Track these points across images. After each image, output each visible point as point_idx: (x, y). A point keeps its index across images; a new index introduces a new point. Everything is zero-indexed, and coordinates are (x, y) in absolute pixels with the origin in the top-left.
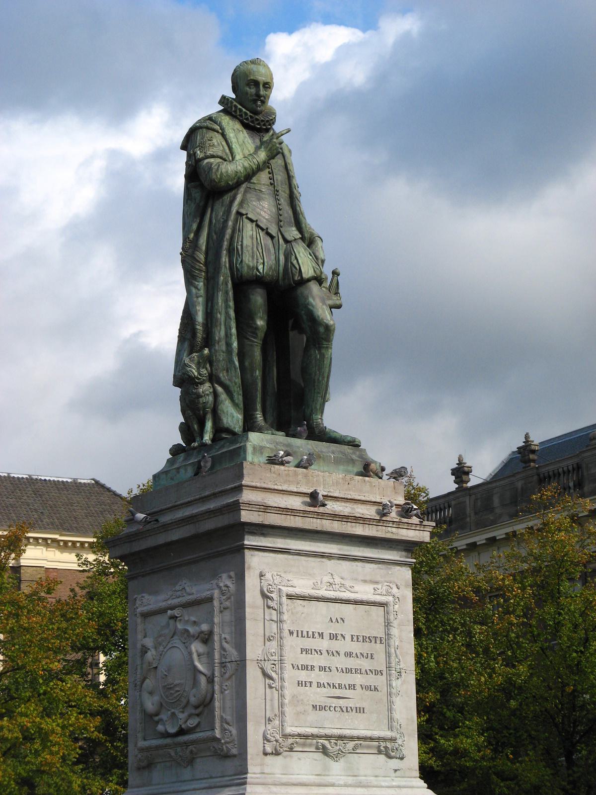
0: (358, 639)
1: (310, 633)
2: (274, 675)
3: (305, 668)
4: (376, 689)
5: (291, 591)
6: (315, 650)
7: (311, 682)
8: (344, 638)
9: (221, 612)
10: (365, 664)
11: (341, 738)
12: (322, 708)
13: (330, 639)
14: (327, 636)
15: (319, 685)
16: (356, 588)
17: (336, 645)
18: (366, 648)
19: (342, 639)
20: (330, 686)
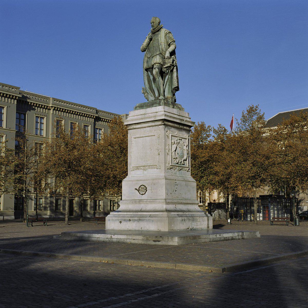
5: (135, 137)
11: (144, 166)
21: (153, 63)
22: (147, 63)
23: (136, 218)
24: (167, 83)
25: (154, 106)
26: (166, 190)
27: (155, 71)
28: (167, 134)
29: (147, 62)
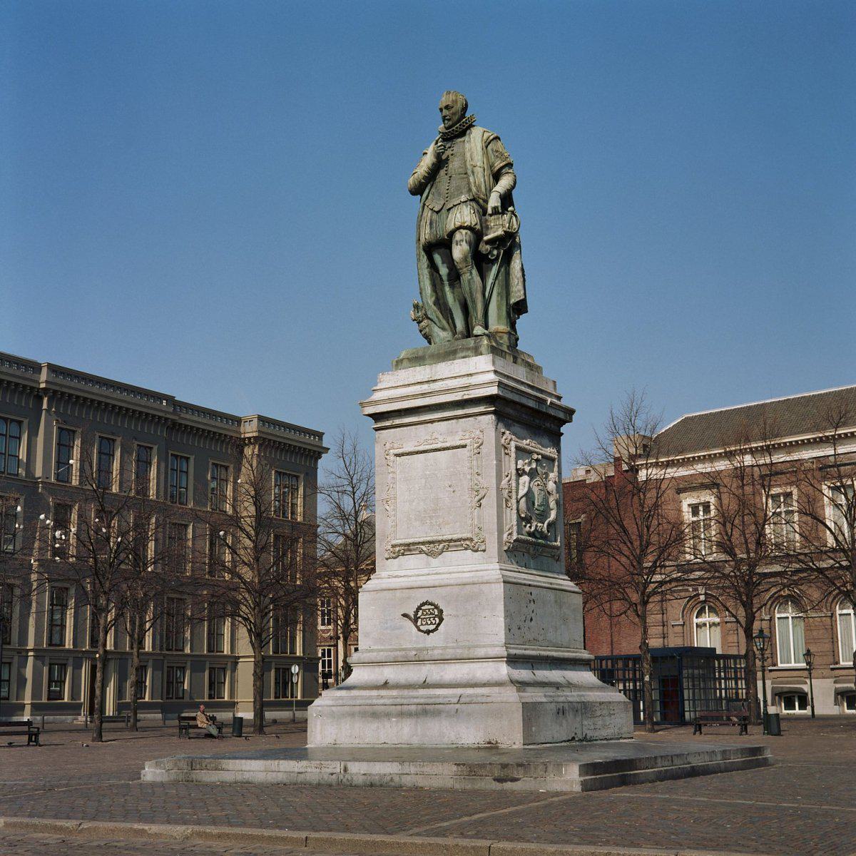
11: (430, 542)
21: (451, 227)
22: (431, 228)
23: (413, 708)
24: (495, 288)
25: (458, 356)
26: (506, 617)
27: (459, 251)
28: (503, 441)
29: (431, 224)
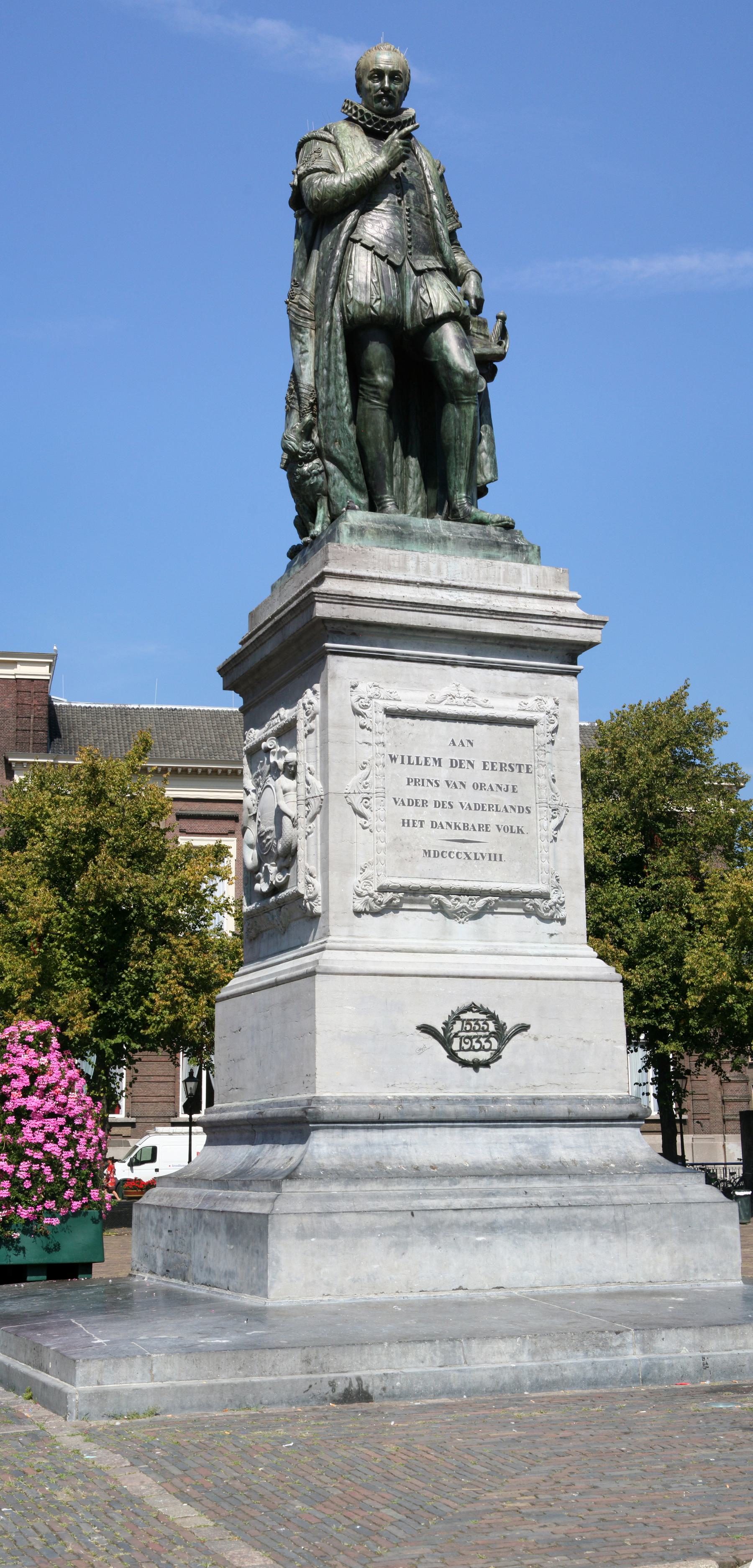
0: (493, 766)
1: (422, 760)
2: (366, 812)
3: (414, 803)
4: (520, 830)
5: (392, 705)
6: (429, 781)
7: (421, 822)
8: (472, 765)
9: (306, 736)
10: (506, 799)
12: (436, 854)
13: (452, 766)
14: (446, 763)
15: (434, 825)
16: (492, 702)
17: (458, 775)
18: (506, 778)
19: (470, 767)
20: (450, 826)
